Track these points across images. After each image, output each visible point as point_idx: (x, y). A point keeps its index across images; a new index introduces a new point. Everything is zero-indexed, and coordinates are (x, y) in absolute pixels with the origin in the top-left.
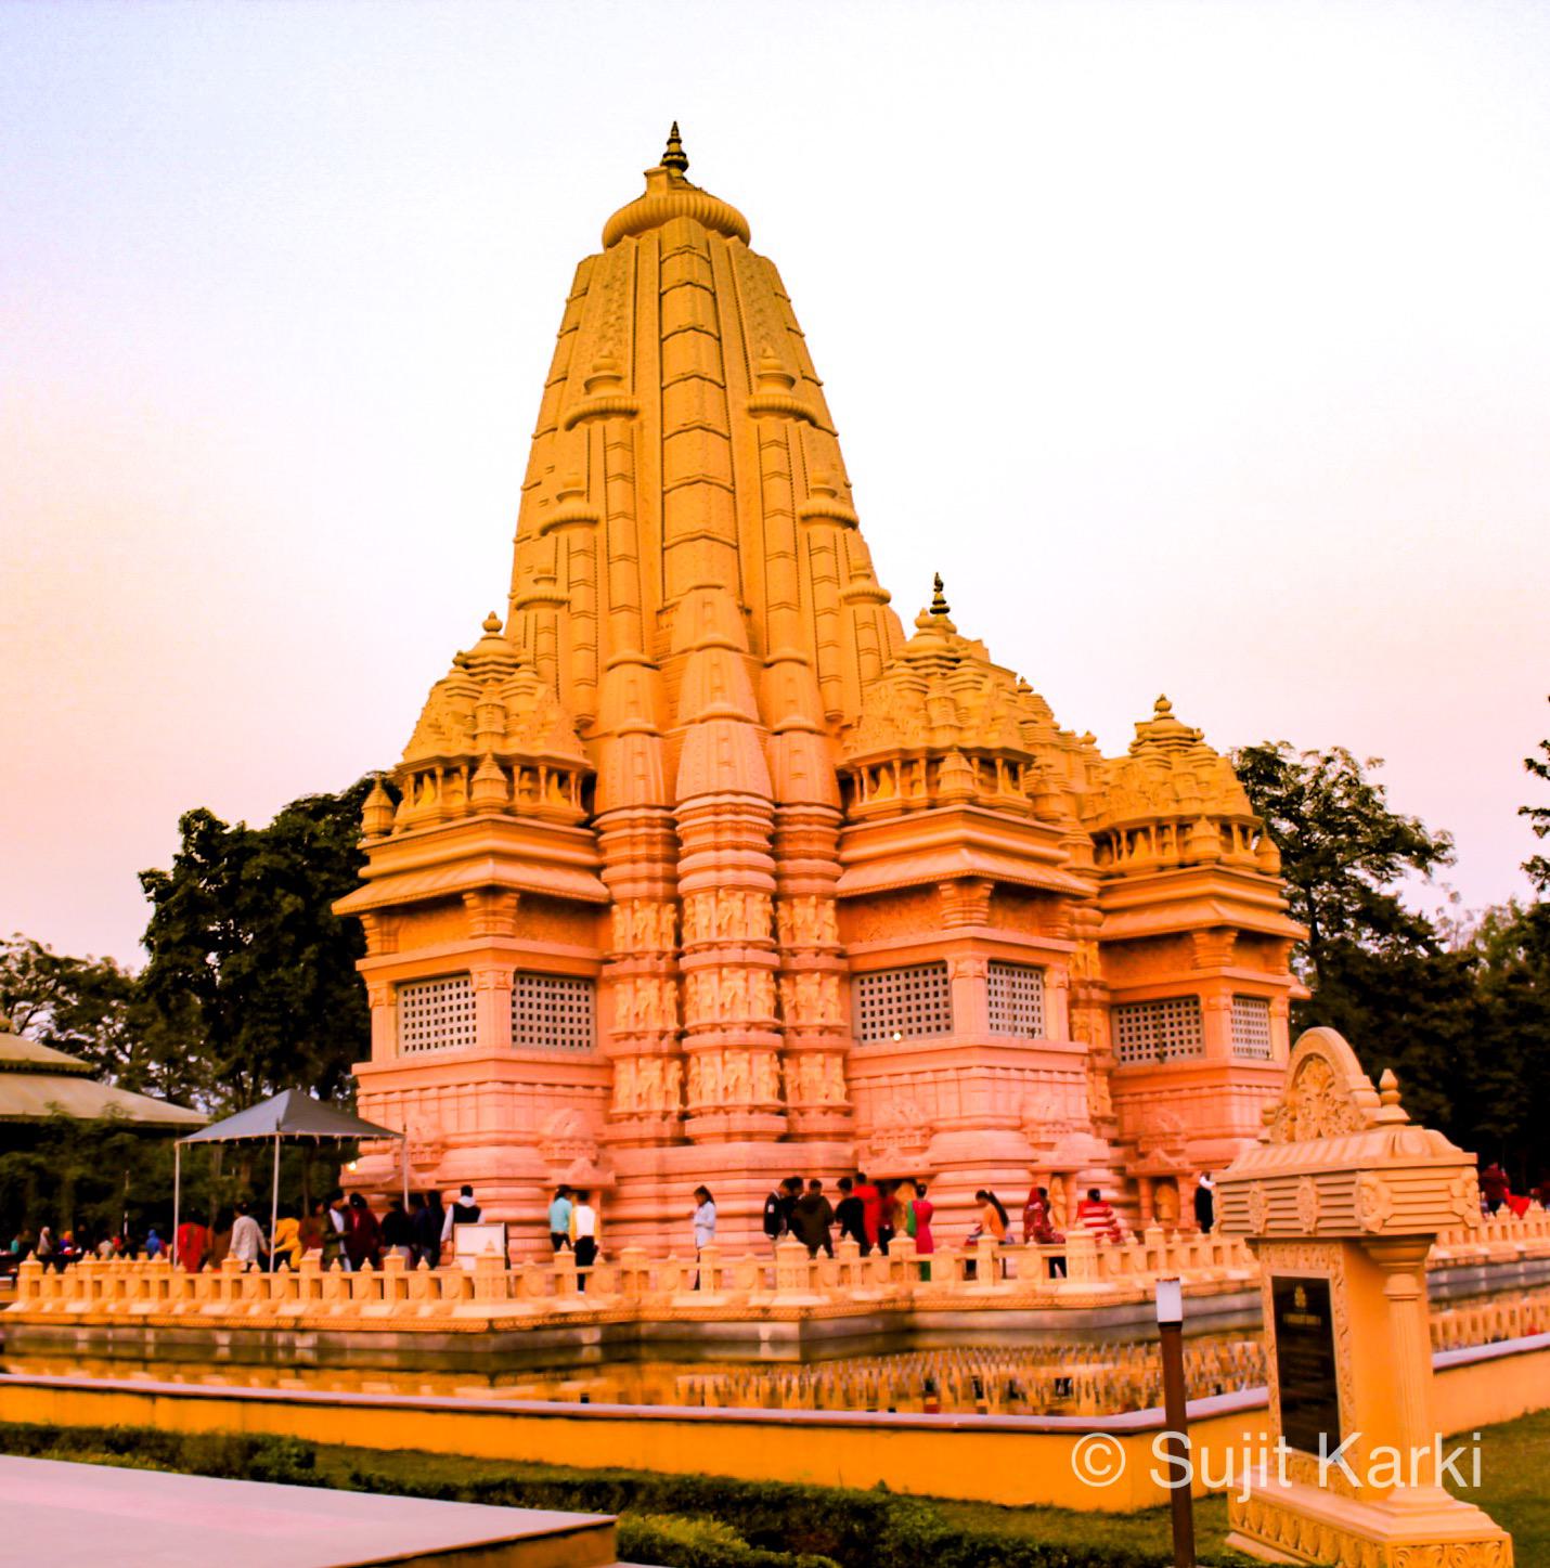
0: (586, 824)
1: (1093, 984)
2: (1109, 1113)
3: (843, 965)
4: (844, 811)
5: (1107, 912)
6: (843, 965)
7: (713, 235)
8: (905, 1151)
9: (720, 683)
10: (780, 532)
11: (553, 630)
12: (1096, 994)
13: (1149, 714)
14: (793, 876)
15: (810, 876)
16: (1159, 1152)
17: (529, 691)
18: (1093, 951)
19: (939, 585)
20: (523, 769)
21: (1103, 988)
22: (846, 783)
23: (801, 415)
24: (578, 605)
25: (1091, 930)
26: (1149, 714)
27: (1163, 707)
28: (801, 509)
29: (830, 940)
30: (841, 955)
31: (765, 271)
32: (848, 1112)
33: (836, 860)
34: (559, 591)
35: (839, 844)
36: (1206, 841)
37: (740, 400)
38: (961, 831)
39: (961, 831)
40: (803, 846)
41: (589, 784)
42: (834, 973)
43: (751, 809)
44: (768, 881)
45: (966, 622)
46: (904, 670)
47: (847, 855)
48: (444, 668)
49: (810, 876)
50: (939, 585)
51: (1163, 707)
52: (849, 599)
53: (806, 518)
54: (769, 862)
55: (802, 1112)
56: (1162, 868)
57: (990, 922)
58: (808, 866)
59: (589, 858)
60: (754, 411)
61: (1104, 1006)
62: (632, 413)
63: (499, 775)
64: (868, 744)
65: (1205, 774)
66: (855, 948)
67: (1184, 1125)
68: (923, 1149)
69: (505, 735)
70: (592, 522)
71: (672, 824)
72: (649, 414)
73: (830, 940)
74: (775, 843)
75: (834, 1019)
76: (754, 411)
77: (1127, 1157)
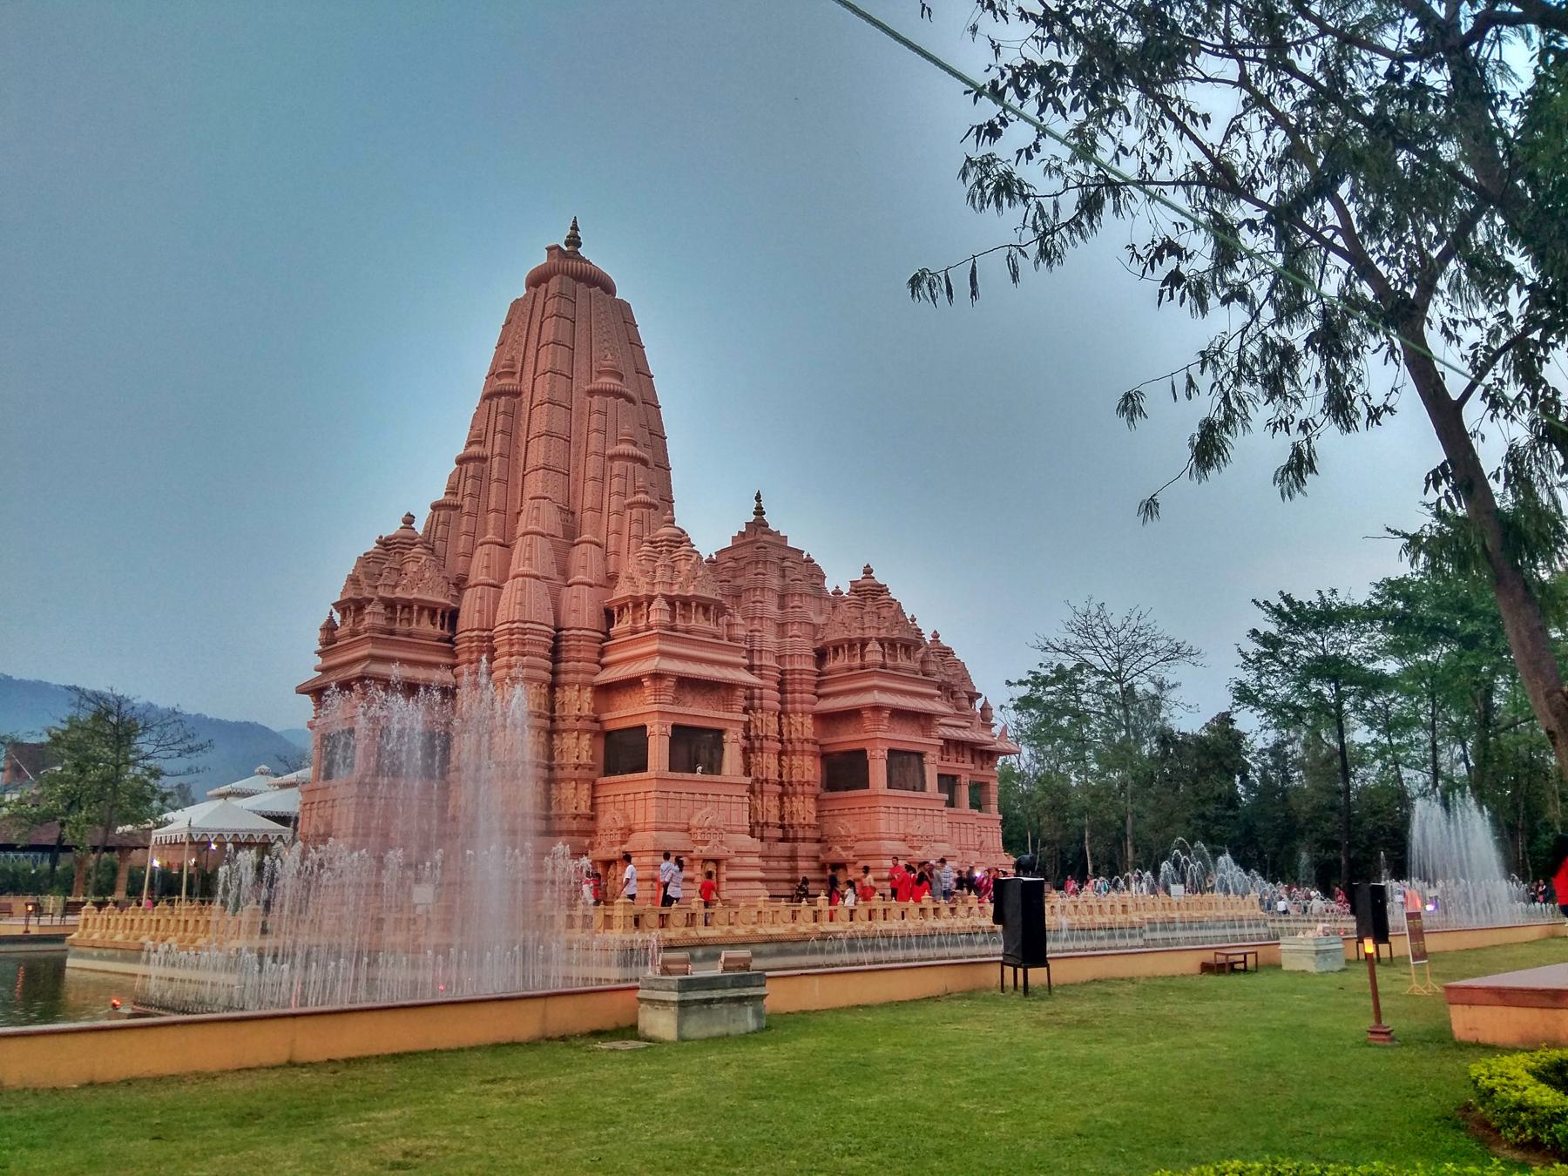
0: (449, 640)
1: (807, 740)
2: (813, 822)
3: (597, 727)
4: (607, 634)
5: (820, 697)
6: (597, 727)
7: (581, 287)
8: (612, 844)
9: (530, 556)
10: (593, 466)
11: (446, 523)
12: (808, 747)
13: (859, 576)
14: (566, 672)
15: (577, 672)
16: (837, 848)
17: (416, 560)
18: (809, 721)
19: (758, 498)
20: (421, 609)
21: (815, 743)
22: (609, 616)
23: (618, 395)
24: (466, 509)
25: (806, 707)
26: (859, 576)
27: (868, 571)
28: (609, 452)
29: (586, 711)
30: (596, 721)
31: (624, 308)
32: (593, 818)
33: (598, 663)
34: (457, 500)
35: (602, 653)
36: (874, 654)
37: (582, 384)
38: (655, 645)
39: (655, 645)
40: (573, 654)
41: (452, 616)
42: (588, 731)
43: (539, 633)
44: (547, 676)
45: (774, 521)
46: (646, 548)
47: (604, 660)
48: (371, 546)
49: (577, 672)
50: (758, 498)
51: (868, 571)
52: (630, 506)
53: (612, 458)
54: (549, 664)
55: (560, 817)
56: (851, 669)
57: (676, 701)
58: (576, 665)
59: (449, 661)
60: (591, 393)
61: (813, 754)
62: (518, 394)
63: (380, 608)
64: (622, 591)
65: (884, 612)
66: (606, 716)
67: (853, 831)
68: (623, 842)
69: (395, 587)
70: (483, 459)
71: (491, 638)
72: (526, 397)
73: (586, 711)
74: (555, 653)
75: (585, 759)
76: (591, 393)
77: (822, 850)
